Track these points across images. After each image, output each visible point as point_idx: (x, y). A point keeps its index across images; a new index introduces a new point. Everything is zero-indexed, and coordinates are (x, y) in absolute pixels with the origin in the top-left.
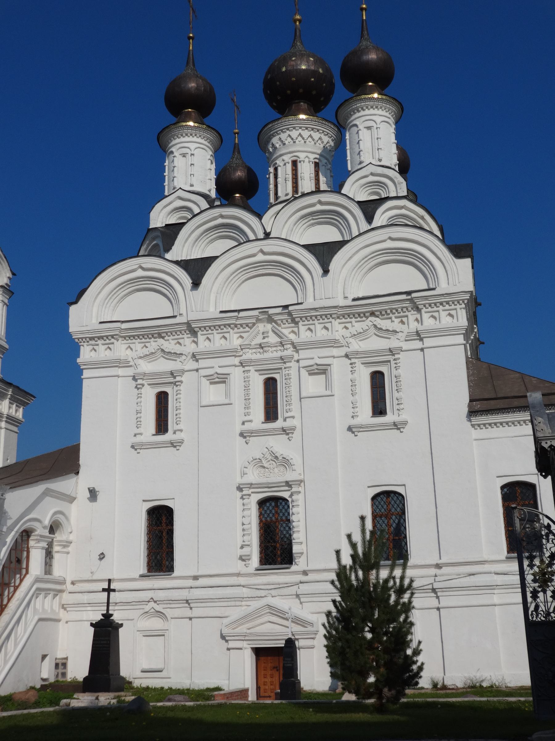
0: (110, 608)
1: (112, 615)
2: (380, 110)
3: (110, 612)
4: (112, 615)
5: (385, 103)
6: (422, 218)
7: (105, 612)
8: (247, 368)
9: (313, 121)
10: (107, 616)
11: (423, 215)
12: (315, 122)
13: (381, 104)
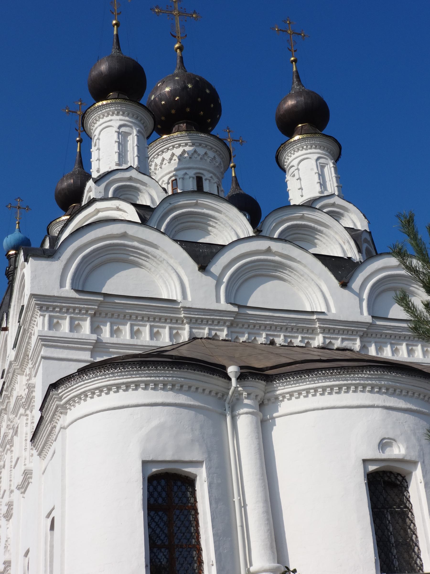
2: (101, 119)
5: (99, 111)
6: (118, 209)
9: (158, 144)
11: (118, 205)
12: (160, 144)
13: (97, 114)
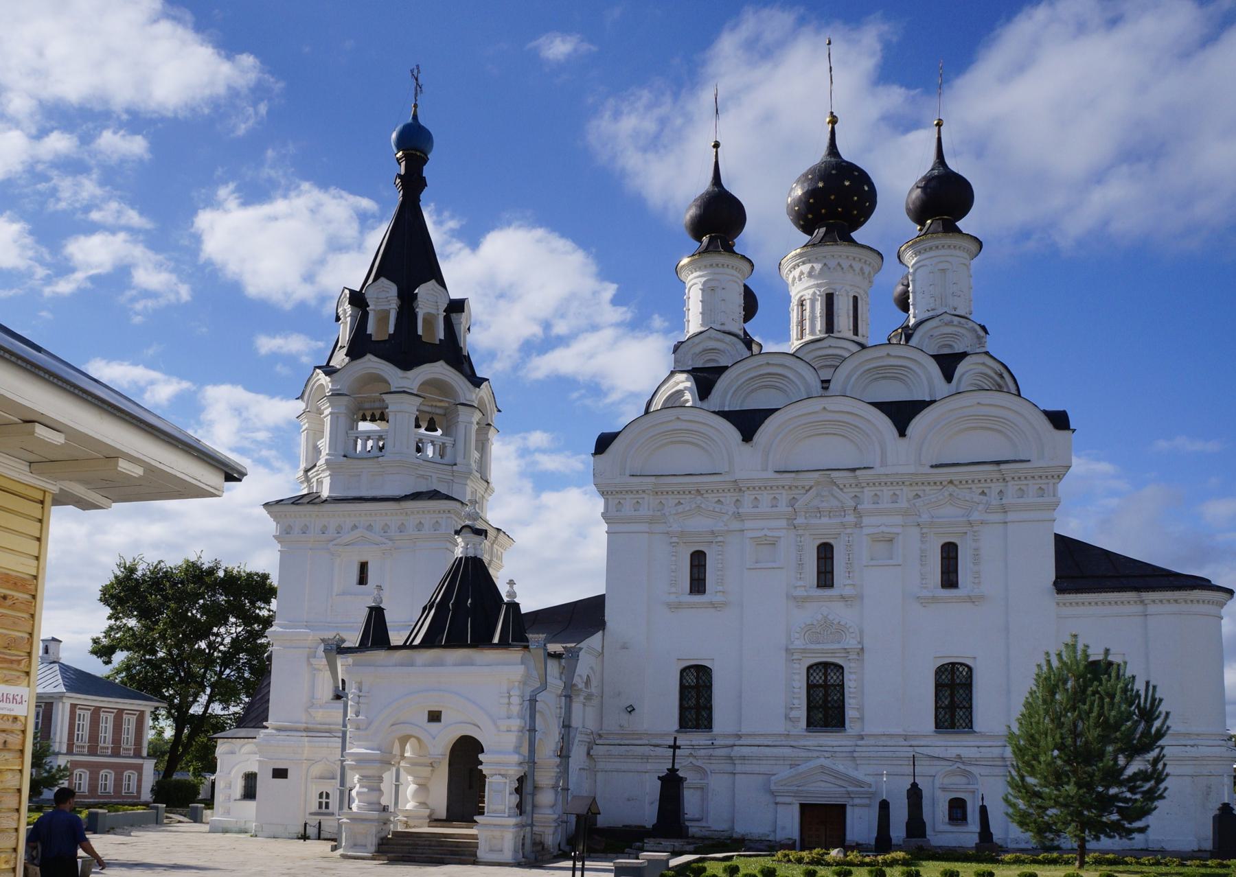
0: (676, 761)
1: (678, 770)
3: (676, 767)
4: (678, 770)
7: (670, 766)
8: (801, 532)
10: (673, 771)
